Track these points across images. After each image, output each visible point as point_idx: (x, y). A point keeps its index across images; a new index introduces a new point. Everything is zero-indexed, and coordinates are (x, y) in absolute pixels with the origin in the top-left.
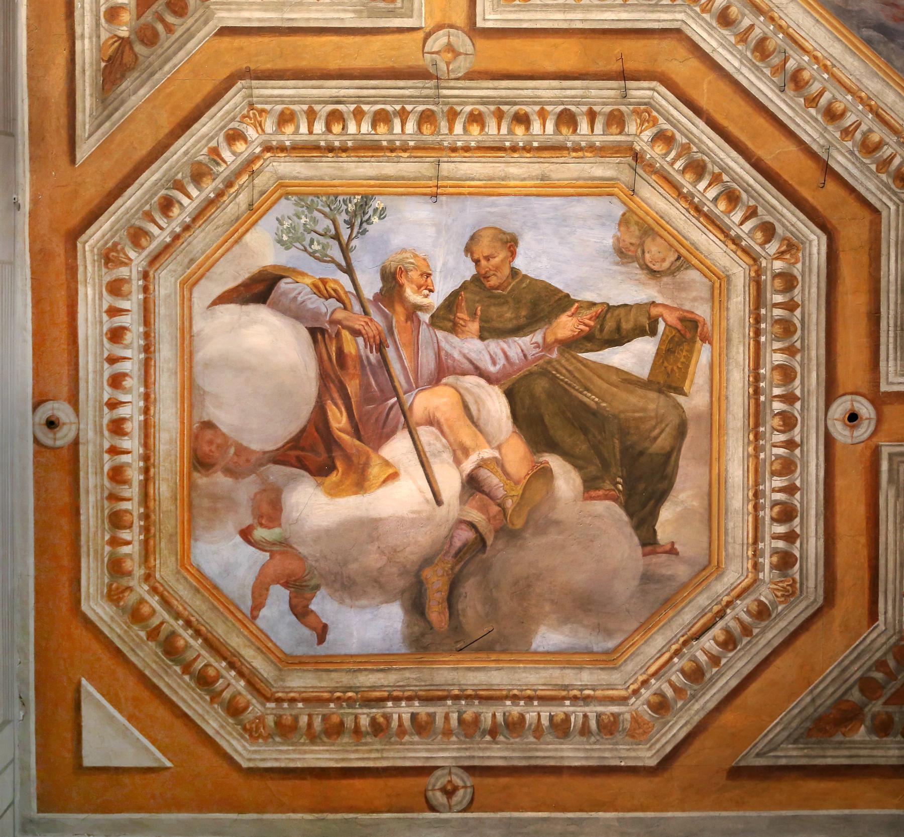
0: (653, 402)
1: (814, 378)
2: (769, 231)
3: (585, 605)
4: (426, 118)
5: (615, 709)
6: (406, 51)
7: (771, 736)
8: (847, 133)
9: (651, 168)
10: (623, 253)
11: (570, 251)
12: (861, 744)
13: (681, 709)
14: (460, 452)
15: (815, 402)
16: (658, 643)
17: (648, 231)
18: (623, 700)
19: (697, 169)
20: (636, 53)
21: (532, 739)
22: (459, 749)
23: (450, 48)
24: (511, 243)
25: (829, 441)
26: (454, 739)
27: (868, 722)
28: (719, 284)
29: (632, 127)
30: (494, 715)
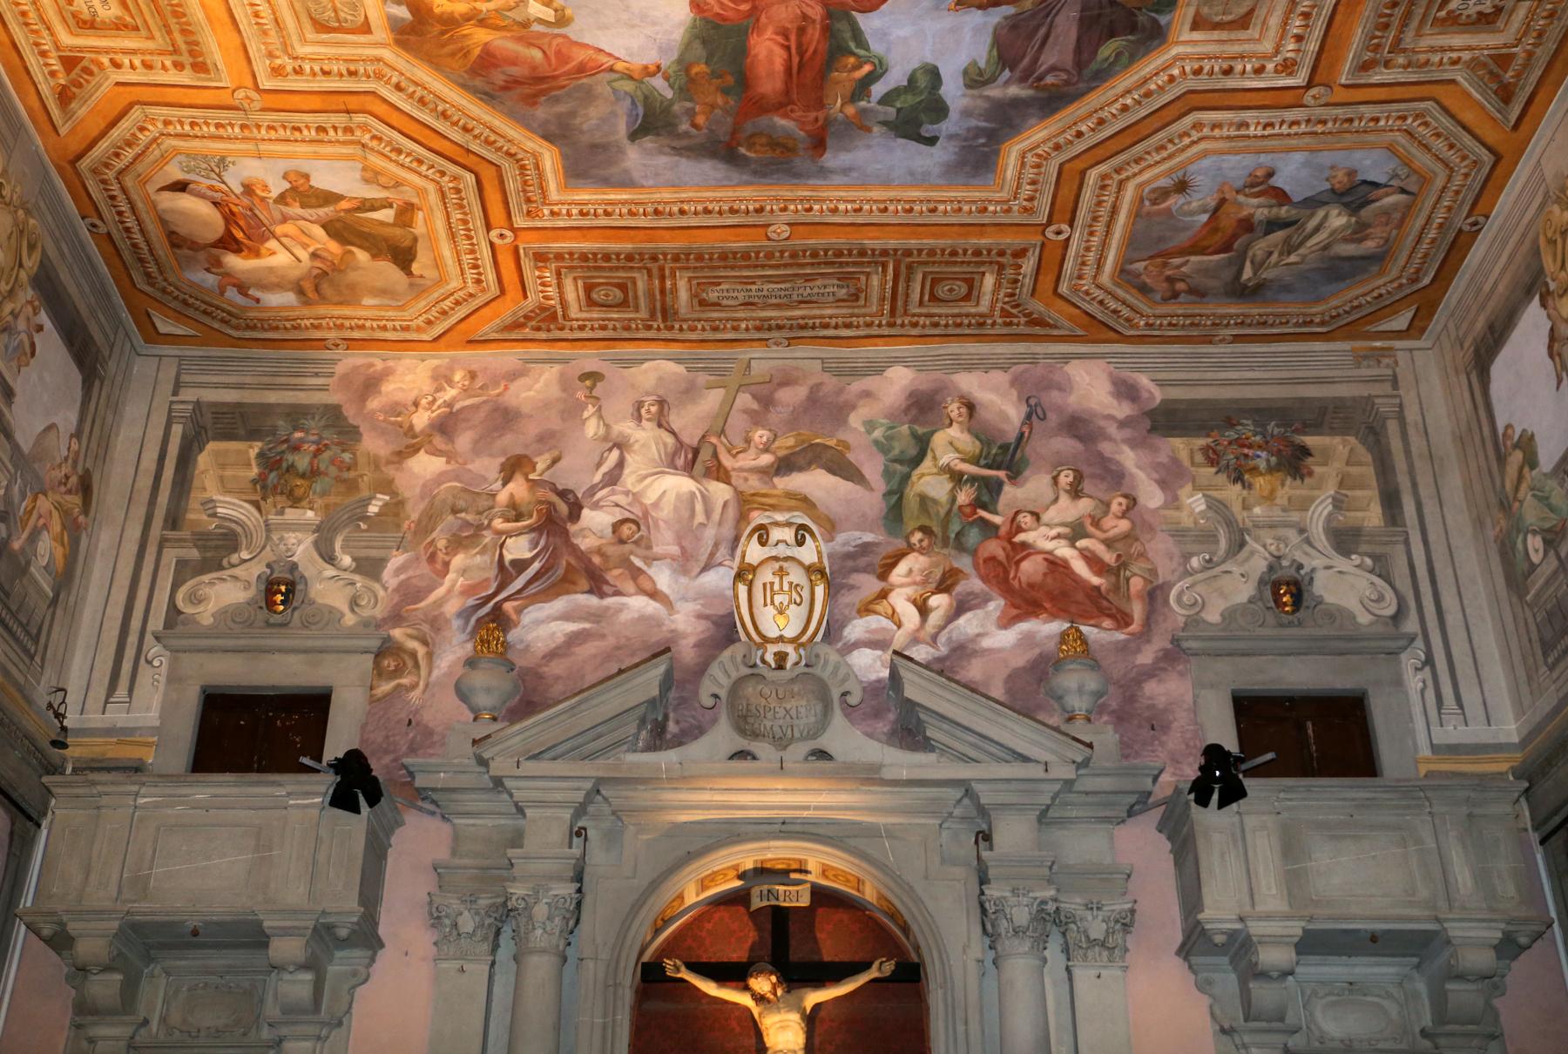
0: (398, 231)
1: (479, 223)
2: (443, 174)
3: (383, 292)
4: (243, 127)
6: (225, 98)
8: (475, 137)
9: (372, 149)
10: (366, 181)
11: (338, 176)
12: (527, 332)
14: (305, 246)
15: (481, 230)
16: (422, 304)
17: (377, 173)
19: (399, 152)
20: (353, 102)
23: (247, 97)
24: (307, 177)
25: (492, 245)
28: (421, 192)
29: (358, 133)
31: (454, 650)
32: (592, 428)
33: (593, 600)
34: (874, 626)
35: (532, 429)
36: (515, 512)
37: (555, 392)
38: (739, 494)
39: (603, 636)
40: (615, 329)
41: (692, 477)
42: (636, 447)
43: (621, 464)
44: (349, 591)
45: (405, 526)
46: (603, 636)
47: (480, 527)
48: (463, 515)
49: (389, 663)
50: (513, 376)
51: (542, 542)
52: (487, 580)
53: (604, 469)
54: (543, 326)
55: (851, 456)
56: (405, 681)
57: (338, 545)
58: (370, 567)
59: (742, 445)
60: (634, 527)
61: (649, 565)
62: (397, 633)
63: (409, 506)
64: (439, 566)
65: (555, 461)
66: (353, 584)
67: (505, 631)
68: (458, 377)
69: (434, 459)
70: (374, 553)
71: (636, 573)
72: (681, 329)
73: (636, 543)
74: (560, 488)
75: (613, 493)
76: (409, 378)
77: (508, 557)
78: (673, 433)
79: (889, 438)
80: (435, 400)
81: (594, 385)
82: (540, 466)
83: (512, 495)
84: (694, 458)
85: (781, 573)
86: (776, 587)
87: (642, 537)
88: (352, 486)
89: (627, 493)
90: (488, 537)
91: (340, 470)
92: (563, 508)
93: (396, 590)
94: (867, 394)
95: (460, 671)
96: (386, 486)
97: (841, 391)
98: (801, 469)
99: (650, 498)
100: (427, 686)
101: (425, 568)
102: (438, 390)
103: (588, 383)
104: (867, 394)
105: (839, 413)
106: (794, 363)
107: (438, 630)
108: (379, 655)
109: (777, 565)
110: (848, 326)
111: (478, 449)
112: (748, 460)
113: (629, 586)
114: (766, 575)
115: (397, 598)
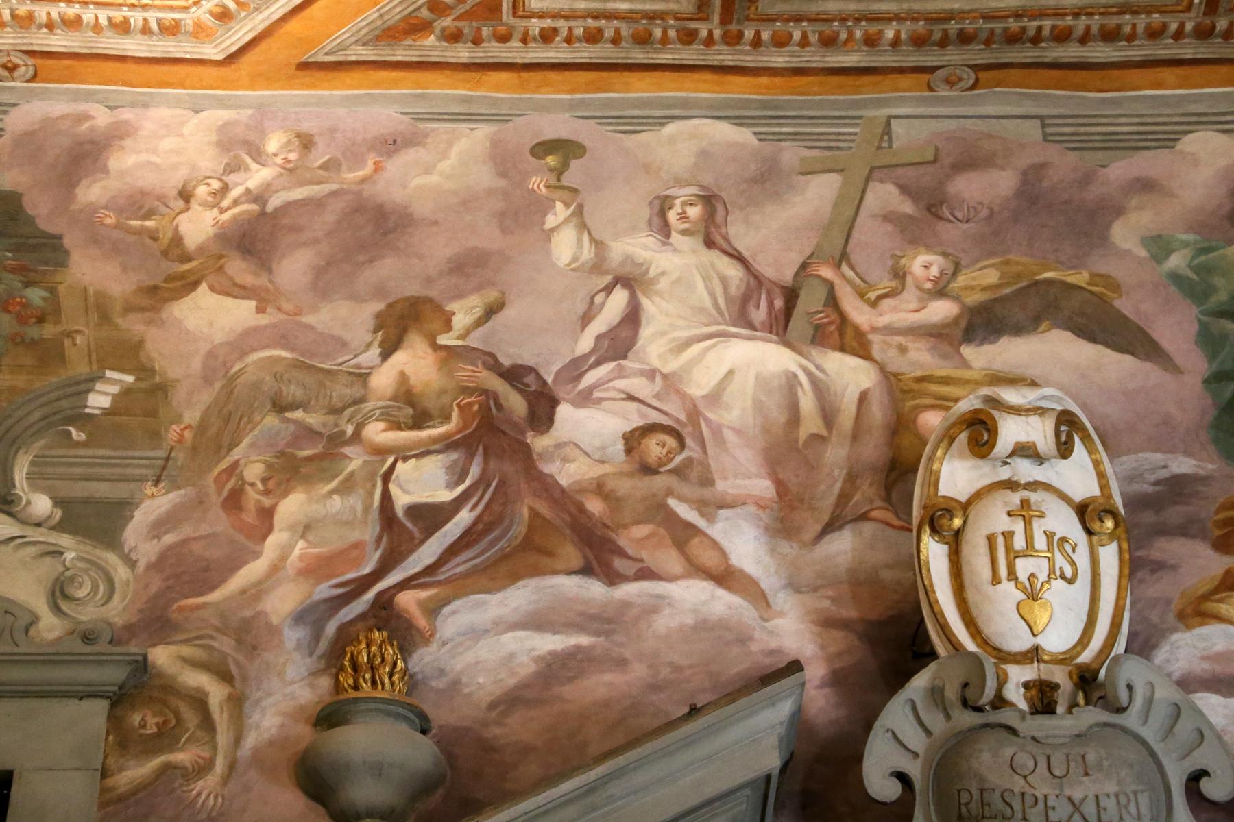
5: (177, 16)
7: (338, 41)
12: (431, 46)
13: (245, 18)
18: (185, 9)
21: (91, 34)
22: (15, 38)
26: (8, 29)
27: (438, 31)
30: (49, 14)
31: (286, 691)
32: (566, 246)
33: (595, 589)
34: (1219, 647)
35: (439, 249)
36: (412, 409)
37: (484, 177)
38: (889, 377)
39: (621, 663)
40: (616, 40)
41: (788, 344)
42: (663, 284)
43: (633, 317)
44: (49, 568)
45: (173, 433)
46: (621, 663)
47: (336, 439)
48: (298, 414)
49: (144, 719)
50: (392, 145)
51: (475, 471)
52: (357, 545)
53: (599, 325)
54: (467, 28)
55: (1124, 305)
56: (181, 757)
57: (20, 474)
58: (96, 520)
59: (887, 283)
60: (671, 442)
61: (711, 519)
62: (162, 656)
63: (179, 396)
64: (250, 517)
65: (492, 311)
66: (57, 553)
67: (405, 651)
68: (273, 143)
69: (229, 302)
70: (101, 490)
71: (682, 534)
72: (757, 42)
73: (676, 472)
74: (506, 362)
75: (621, 374)
76: (167, 144)
77: (402, 500)
78: (739, 258)
79: (1205, 270)
80: (225, 189)
81: (565, 166)
82: (461, 320)
83: (403, 377)
84: (784, 307)
85: (1026, 512)
86: (1019, 543)
87: (689, 462)
88: (50, 355)
89: (651, 374)
90: (355, 460)
91: (22, 320)
92: (516, 403)
93: (158, 564)
94: (1146, 186)
95: (304, 733)
96: (128, 353)
97: (1087, 179)
98: (1018, 330)
99: (700, 384)
100: (232, 766)
101: (218, 522)
102: (232, 168)
103: (551, 160)
104: (1146, 186)
105: (1089, 222)
106: (982, 126)
107: (253, 649)
108: (120, 699)
109: (1015, 498)
110: (1110, 36)
111: (324, 283)
112: (902, 311)
113: (670, 560)
114: (996, 517)
115: (156, 584)
